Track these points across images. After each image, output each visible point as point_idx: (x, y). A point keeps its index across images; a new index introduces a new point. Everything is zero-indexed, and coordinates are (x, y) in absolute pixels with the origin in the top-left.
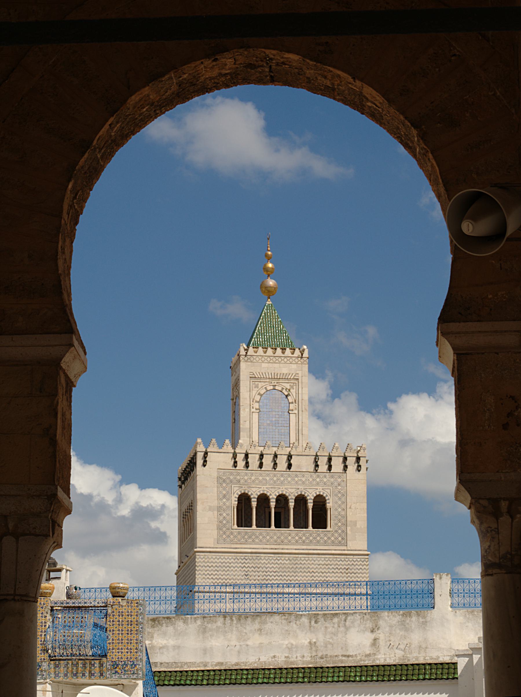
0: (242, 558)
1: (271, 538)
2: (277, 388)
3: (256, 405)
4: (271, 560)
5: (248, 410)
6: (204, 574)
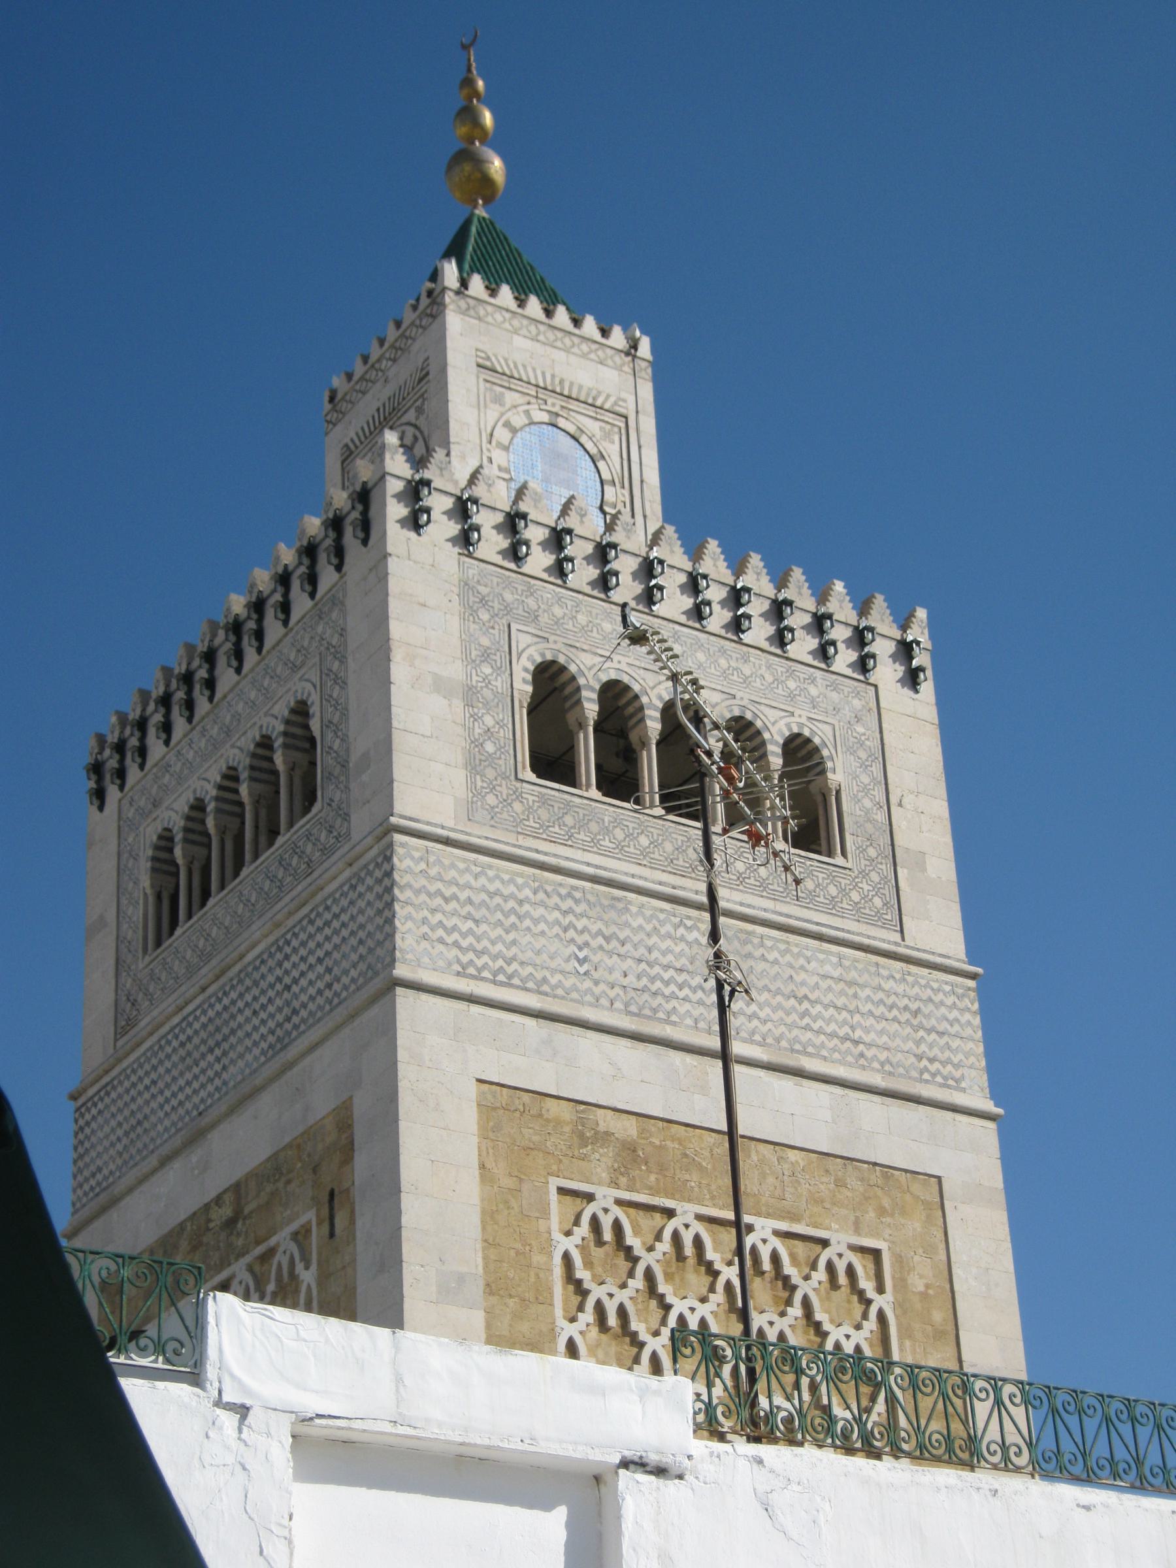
0: (563, 891)
2: (561, 422)
4: (662, 923)
6: (425, 921)
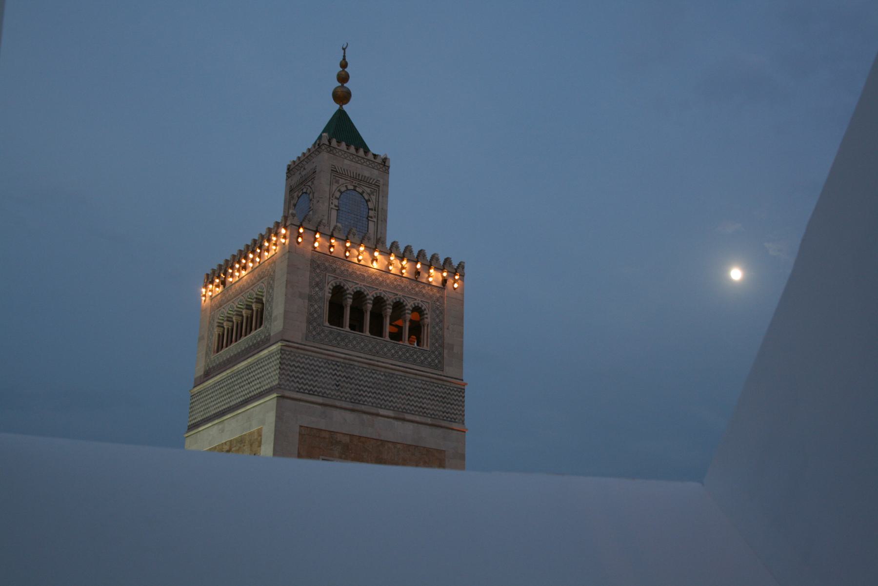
1: (366, 345)
2: (357, 189)
3: (336, 202)
5: (326, 204)
